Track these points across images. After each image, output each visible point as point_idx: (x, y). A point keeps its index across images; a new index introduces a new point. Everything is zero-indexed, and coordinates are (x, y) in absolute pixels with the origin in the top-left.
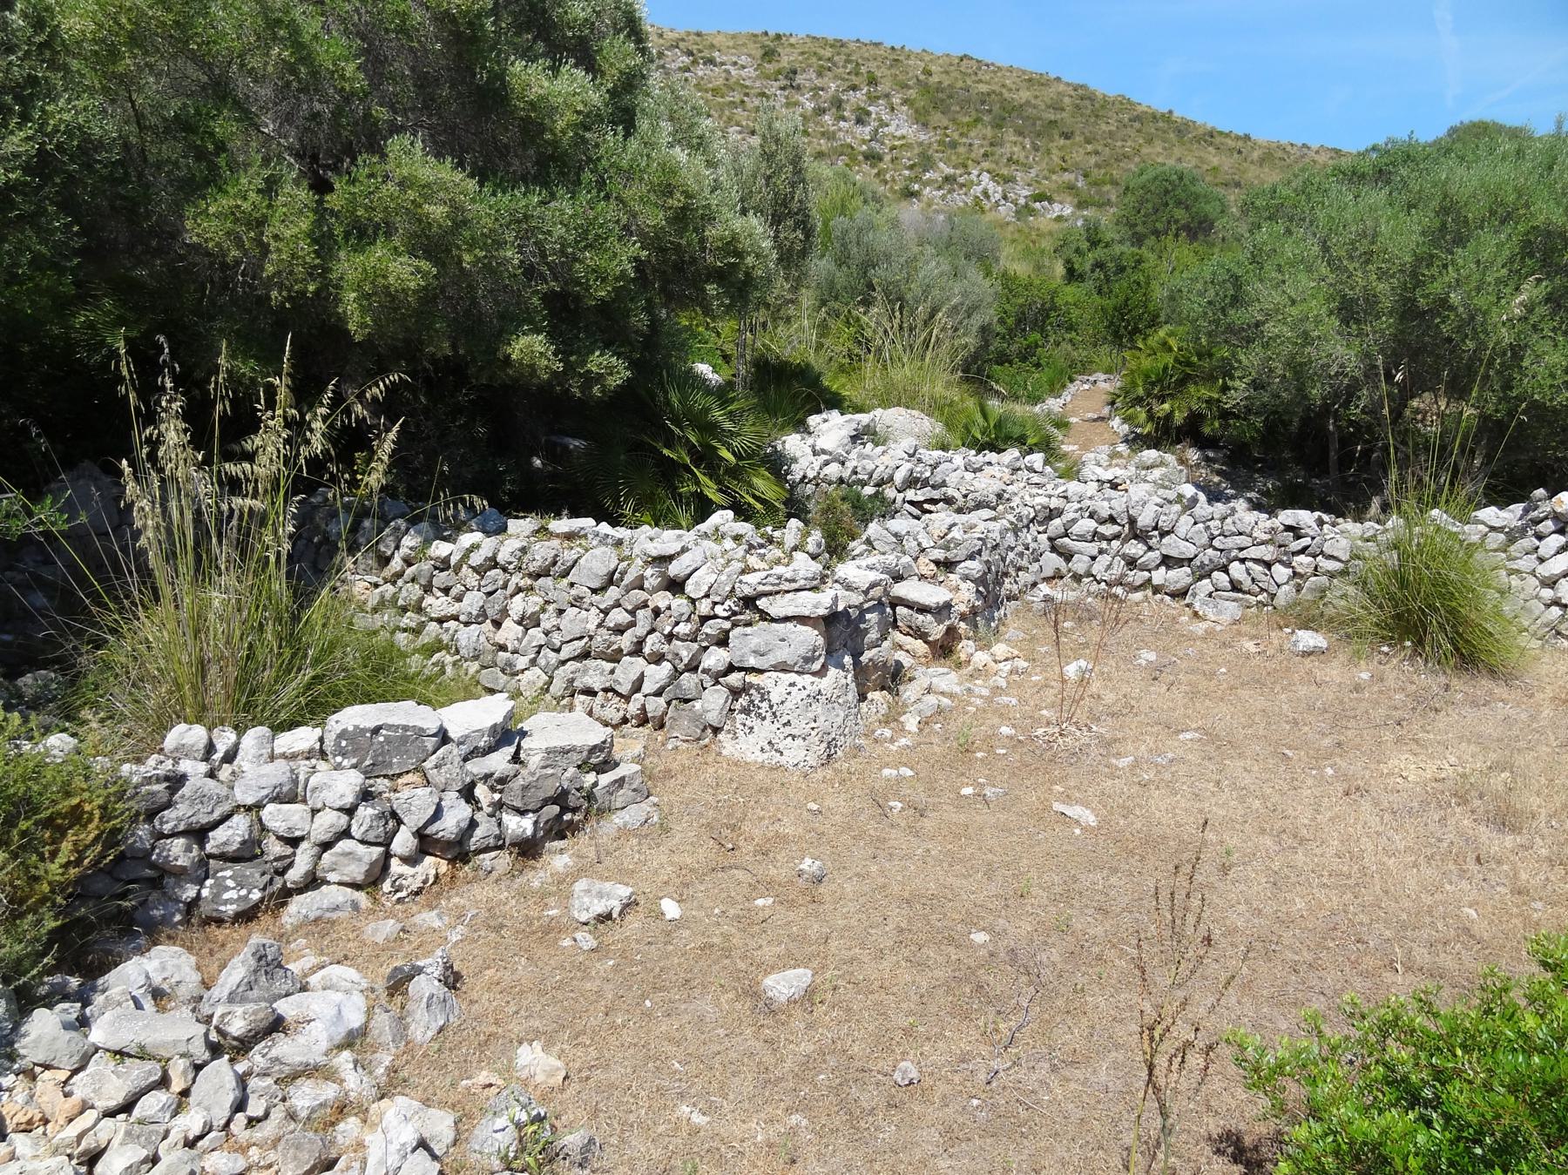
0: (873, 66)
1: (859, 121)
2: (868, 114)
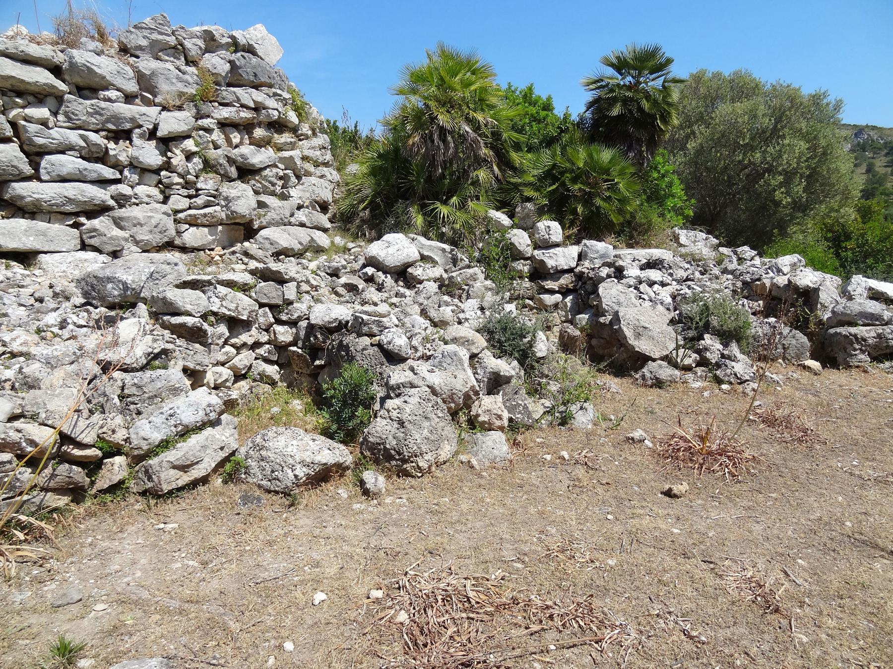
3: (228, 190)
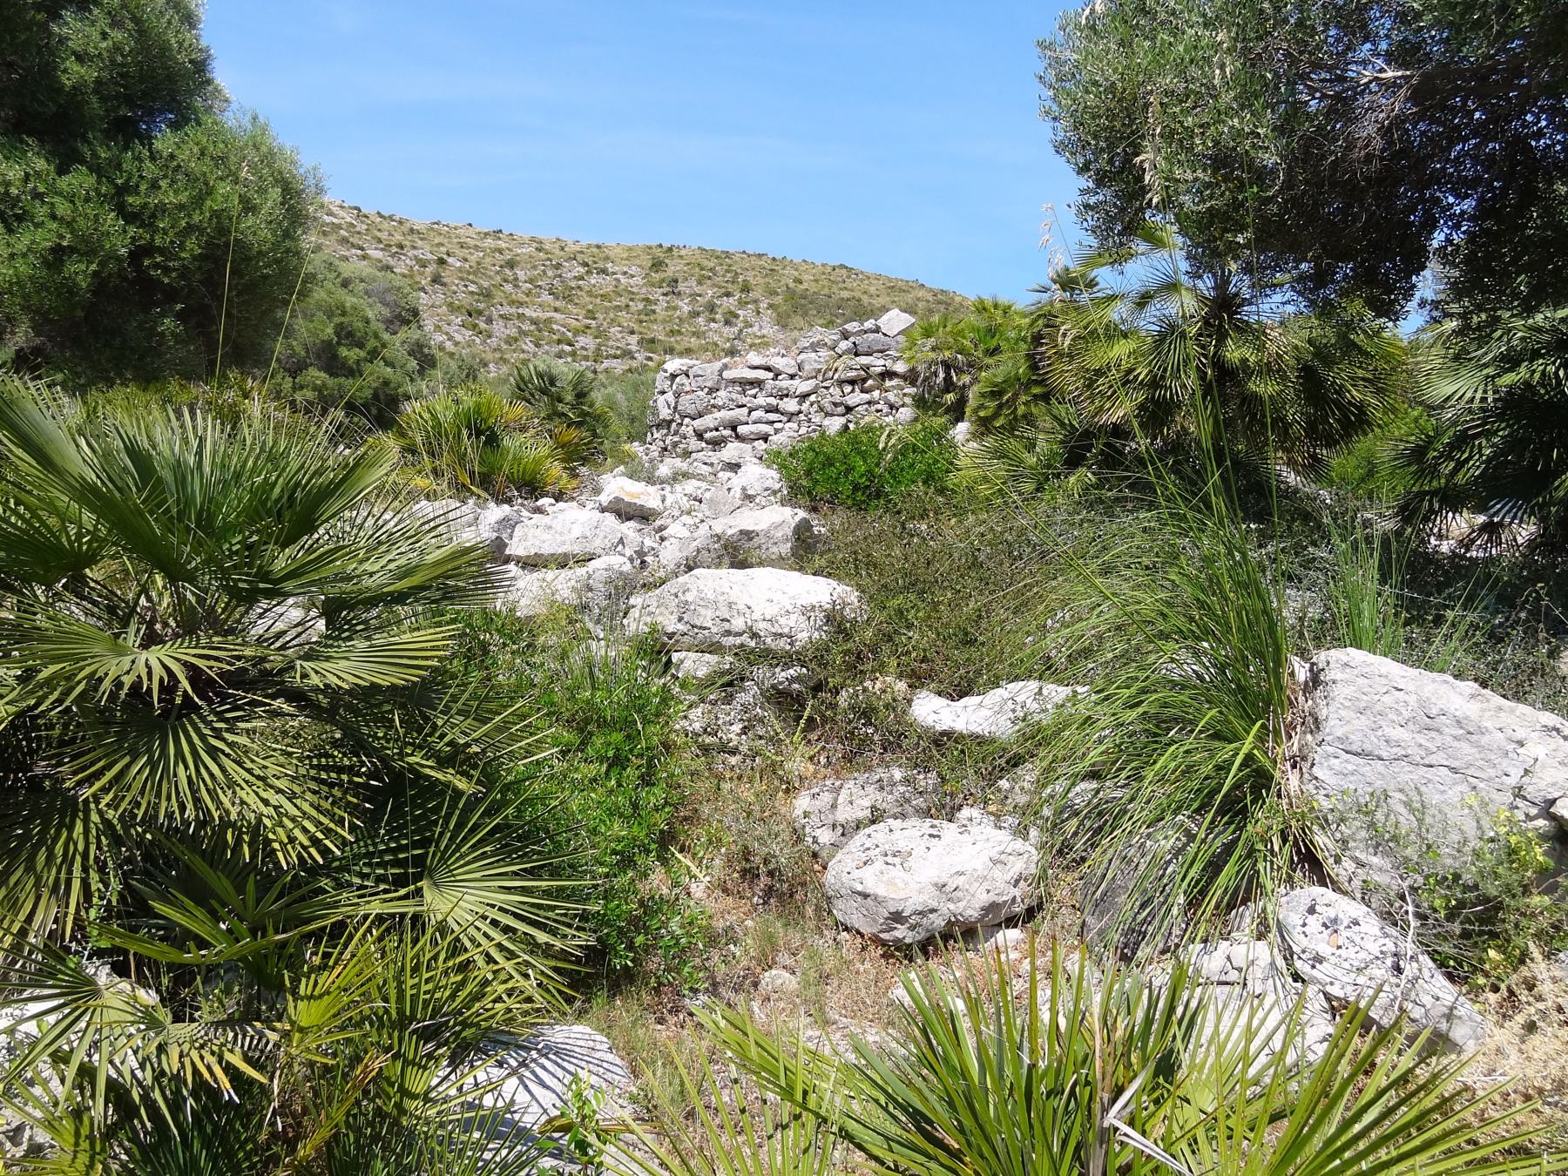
0: (750, 277)
1: (727, 323)
2: (737, 316)
3: (826, 422)
